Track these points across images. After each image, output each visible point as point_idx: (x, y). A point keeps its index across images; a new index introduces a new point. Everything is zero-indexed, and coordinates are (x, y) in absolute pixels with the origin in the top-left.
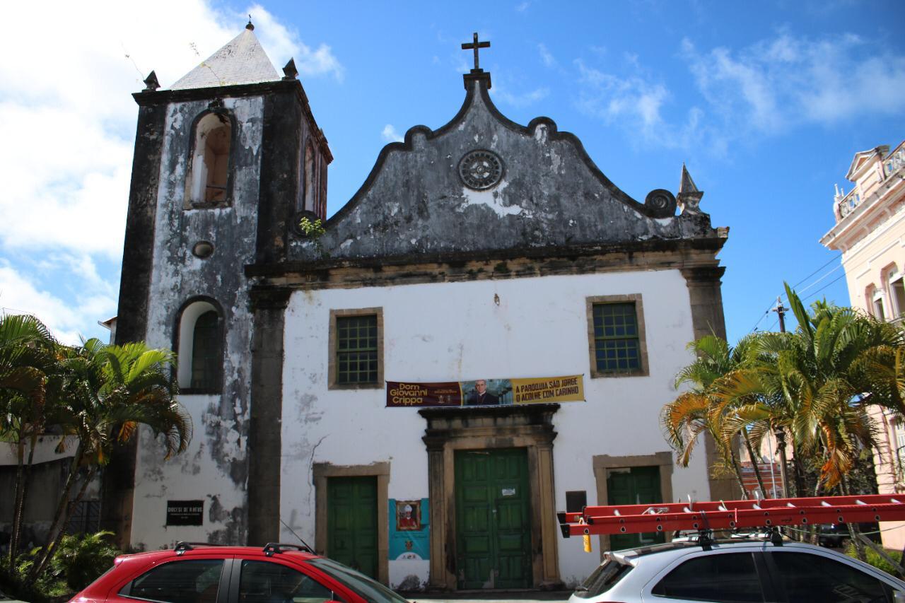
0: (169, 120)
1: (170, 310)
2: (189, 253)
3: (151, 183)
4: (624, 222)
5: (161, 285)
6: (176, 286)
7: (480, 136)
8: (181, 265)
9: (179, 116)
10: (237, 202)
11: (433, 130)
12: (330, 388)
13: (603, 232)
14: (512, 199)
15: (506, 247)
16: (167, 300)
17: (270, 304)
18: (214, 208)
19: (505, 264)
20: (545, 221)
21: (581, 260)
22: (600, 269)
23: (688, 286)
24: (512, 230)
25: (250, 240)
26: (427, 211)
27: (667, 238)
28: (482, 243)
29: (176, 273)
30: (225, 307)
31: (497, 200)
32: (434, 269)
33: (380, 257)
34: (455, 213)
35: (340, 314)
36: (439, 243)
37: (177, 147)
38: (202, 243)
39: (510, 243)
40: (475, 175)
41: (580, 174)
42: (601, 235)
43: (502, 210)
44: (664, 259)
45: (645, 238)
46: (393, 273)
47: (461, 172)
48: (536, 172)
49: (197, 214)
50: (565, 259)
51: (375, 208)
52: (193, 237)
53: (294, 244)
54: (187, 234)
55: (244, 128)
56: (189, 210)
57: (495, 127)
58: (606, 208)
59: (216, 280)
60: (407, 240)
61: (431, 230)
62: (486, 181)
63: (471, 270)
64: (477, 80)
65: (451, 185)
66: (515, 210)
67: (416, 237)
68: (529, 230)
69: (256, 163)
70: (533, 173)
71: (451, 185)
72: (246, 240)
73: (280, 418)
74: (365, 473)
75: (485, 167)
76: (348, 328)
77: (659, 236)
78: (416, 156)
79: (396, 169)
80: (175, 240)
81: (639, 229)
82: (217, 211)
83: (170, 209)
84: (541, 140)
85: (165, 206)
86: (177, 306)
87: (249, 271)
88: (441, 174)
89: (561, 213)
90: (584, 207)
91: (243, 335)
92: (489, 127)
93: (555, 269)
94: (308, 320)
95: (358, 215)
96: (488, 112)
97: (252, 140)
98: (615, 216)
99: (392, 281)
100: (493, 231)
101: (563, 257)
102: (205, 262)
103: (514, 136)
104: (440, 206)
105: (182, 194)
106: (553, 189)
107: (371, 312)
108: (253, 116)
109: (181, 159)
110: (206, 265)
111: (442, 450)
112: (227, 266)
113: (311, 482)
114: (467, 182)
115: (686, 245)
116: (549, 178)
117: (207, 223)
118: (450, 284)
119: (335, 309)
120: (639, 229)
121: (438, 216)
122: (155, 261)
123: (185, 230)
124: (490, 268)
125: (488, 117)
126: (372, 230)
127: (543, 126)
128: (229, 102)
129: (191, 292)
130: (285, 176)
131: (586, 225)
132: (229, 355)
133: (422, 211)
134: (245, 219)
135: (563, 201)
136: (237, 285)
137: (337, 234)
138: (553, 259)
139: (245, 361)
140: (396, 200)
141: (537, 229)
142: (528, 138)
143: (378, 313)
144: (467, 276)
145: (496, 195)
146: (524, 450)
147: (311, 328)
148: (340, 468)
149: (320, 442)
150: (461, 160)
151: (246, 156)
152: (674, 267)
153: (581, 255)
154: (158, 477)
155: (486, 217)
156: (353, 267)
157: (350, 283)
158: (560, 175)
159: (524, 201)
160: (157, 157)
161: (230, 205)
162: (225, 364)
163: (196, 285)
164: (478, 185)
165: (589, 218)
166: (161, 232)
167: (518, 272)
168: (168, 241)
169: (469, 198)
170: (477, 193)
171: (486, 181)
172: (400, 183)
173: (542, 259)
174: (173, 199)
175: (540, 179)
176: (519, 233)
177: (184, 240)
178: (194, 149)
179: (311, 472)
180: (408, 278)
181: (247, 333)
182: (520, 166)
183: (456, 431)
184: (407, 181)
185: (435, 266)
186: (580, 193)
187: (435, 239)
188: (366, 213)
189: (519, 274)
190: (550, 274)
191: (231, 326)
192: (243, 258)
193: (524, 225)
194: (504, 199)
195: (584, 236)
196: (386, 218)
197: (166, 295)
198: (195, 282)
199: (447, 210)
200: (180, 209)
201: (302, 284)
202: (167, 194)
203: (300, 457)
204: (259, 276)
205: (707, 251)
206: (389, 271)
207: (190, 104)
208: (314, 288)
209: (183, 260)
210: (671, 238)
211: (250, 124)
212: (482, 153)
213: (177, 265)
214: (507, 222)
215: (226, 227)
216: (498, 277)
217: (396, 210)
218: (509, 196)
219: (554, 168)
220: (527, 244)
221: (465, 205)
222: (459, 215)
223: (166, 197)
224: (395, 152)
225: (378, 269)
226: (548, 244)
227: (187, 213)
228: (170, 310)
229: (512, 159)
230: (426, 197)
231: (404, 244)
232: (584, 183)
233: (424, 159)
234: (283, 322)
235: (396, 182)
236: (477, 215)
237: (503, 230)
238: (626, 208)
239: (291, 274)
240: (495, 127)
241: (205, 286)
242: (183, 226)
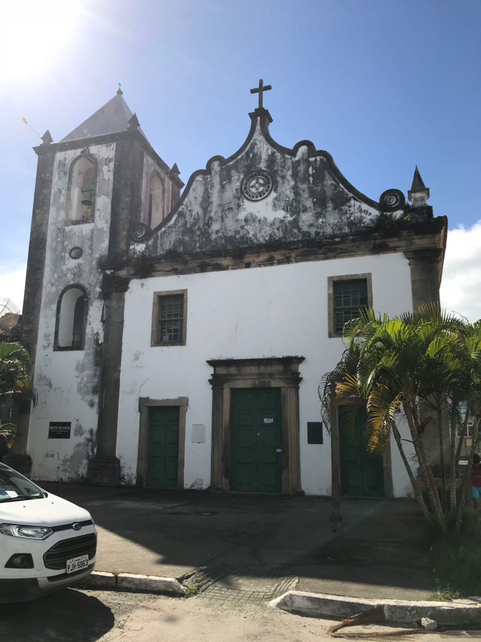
11: (226, 157)
12: (152, 346)
17: (114, 289)
73: (120, 366)
74: (171, 404)
94: (140, 300)
107: (180, 293)
111: (223, 389)
113: (137, 410)
130: (128, 199)
143: (185, 294)
146: (279, 389)
148: (156, 401)
149: (144, 382)
152: (400, 251)
179: (138, 402)
180: (203, 268)
183: (231, 375)
203: (132, 392)
225: (186, 262)
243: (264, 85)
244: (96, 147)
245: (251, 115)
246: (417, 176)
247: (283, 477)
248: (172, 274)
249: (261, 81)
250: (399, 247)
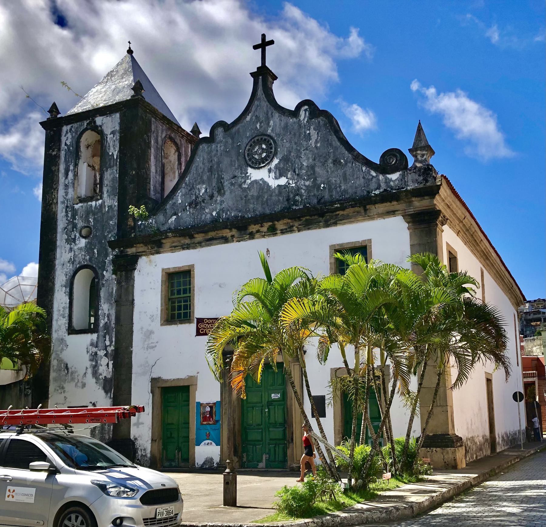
1: (68, 276)
2: (78, 235)
3: (54, 187)
4: (362, 180)
5: (62, 259)
6: (71, 259)
7: (260, 124)
8: (73, 244)
10: (105, 195)
11: (229, 123)
13: (345, 191)
14: (281, 172)
15: (275, 212)
16: (66, 270)
17: (126, 267)
18: (91, 202)
19: (274, 225)
20: (304, 188)
21: (327, 216)
22: (340, 222)
23: (409, 229)
24: (280, 198)
26: (223, 189)
27: (395, 190)
28: (259, 209)
29: (71, 250)
30: (99, 272)
31: (271, 174)
32: (227, 233)
33: (193, 227)
34: (242, 188)
35: (168, 271)
36: (231, 213)
37: (69, 159)
38: (85, 227)
39: (278, 208)
40: (256, 157)
41: (331, 145)
42: (344, 194)
43: (273, 183)
44: (392, 208)
45: (377, 192)
46: (201, 238)
47: (246, 155)
48: (299, 148)
49: (82, 207)
50: (316, 217)
51: (190, 191)
52: (80, 224)
53: (140, 222)
54: (76, 221)
55: (108, 139)
56: (77, 204)
57: (272, 113)
58: (349, 171)
59: (94, 253)
60: (211, 212)
61: (225, 204)
62: (263, 160)
63: (252, 232)
65: (240, 167)
66: (283, 181)
67: (216, 210)
68: (291, 196)
70: (297, 149)
71: (240, 167)
75: (263, 149)
76: (176, 281)
77: (388, 189)
78: (217, 147)
79: (204, 159)
80: (70, 227)
81: (373, 185)
82: (93, 203)
84: (304, 120)
85: (63, 203)
86: (72, 273)
87: (113, 245)
88: (234, 159)
89: (315, 179)
90: (332, 172)
91: (110, 291)
92: (267, 114)
93: (308, 225)
95: (179, 197)
96: (267, 103)
98: (355, 176)
99: (200, 244)
100: (267, 199)
101: (314, 215)
102: (87, 240)
104: (232, 184)
105: (73, 193)
106: (311, 160)
107: (187, 268)
108: (113, 129)
109: (71, 168)
112: (100, 243)
114: (250, 163)
115: (406, 195)
116: (308, 152)
117: (89, 212)
118: (237, 243)
119: (165, 268)
120: (373, 185)
121: (231, 193)
122: (58, 243)
124: (265, 229)
125: (267, 106)
126: (188, 208)
127: (306, 107)
129: (79, 263)
131: (333, 187)
132: (102, 305)
133: (220, 190)
134: (110, 207)
135: (317, 169)
136: (107, 255)
137: (166, 213)
138: (307, 218)
139: (112, 309)
140: (203, 183)
141: (297, 195)
142: (295, 119)
144: (248, 236)
145: (270, 171)
147: (150, 283)
150: (247, 145)
151: (110, 160)
153: (327, 212)
155: (263, 189)
156: (174, 237)
157: (174, 248)
158: (316, 147)
159: (290, 173)
160: (57, 168)
161: (101, 198)
162: (100, 312)
163: (82, 257)
164: (257, 165)
165: (335, 181)
166: (61, 223)
167: (281, 230)
168: (66, 228)
169: (251, 175)
170: (257, 171)
171: (266, 159)
172: (206, 170)
173: (299, 218)
174: (67, 197)
175: (301, 153)
176: (285, 199)
177: (75, 226)
178: (79, 159)
180: (210, 241)
181: (113, 289)
182: (288, 145)
184: (211, 167)
185: (228, 231)
186: (330, 161)
187: (228, 210)
188: (184, 195)
189: (283, 232)
190: (305, 230)
191: (103, 284)
192: (110, 236)
193: (288, 193)
194: (275, 173)
195: (331, 196)
196: (197, 197)
197: (65, 266)
199: (236, 187)
201: (144, 252)
204: (119, 248)
205: (426, 198)
206: (199, 237)
208: (153, 254)
209: (74, 240)
210: (398, 189)
211: (112, 135)
212: (263, 138)
214: (277, 191)
215: (99, 214)
216: (269, 236)
217: (203, 191)
218: (279, 170)
219: (312, 142)
220: (290, 208)
221: (249, 181)
222: (245, 190)
223: (63, 196)
224: (204, 145)
225: (192, 237)
226: (305, 206)
227: (76, 207)
228: (68, 276)
229: (282, 140)
230: (223, 178)
231: (208, 216)
232: (334, 152)
233: (222, 148)
234: (134, 280)
235: (204, 169)
236: (257, 188)
237: (274, 198)
238: (364, 169)
239: (138, 245)
240: (272, 113)
241: (88, 257)
242: (74, 217)
243: (267, 40)
244: (101, 118)
245: (252, 74)
246: (420, 130)
247: (289, 452)
248: (179, 250)
249: (264, 36)
250: (397, 211)
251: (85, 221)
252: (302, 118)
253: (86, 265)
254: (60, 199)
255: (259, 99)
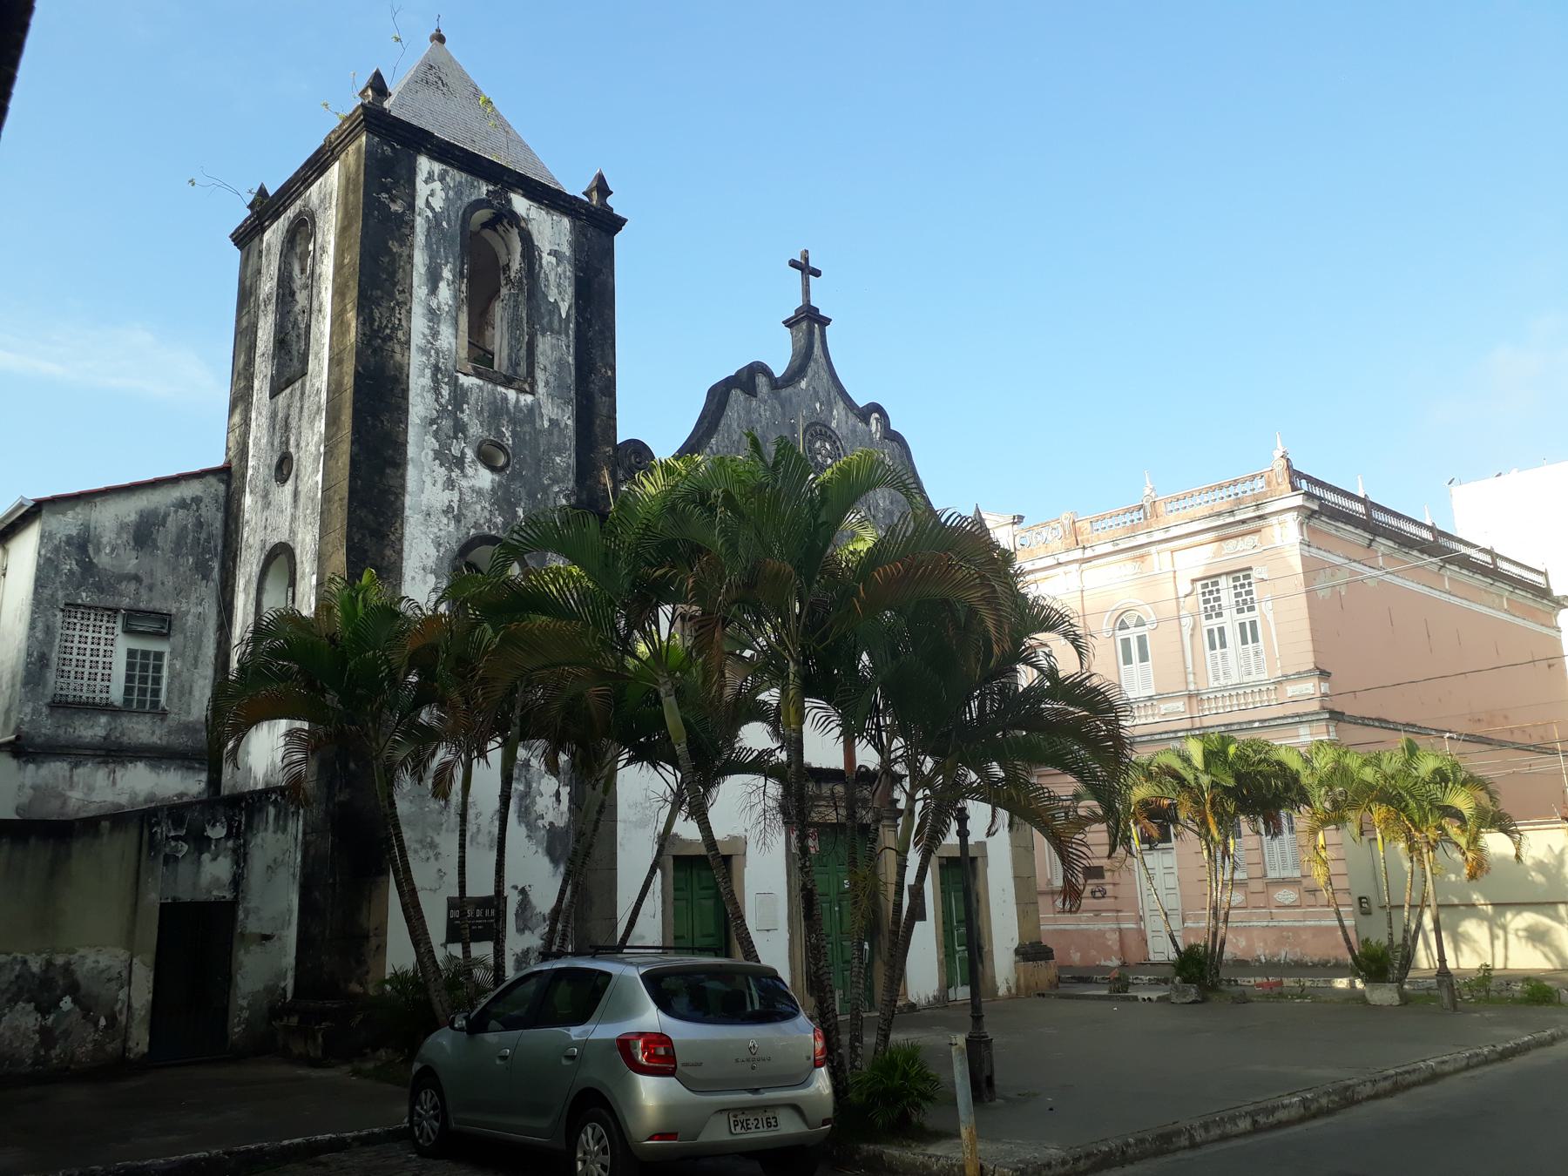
0: (422, 190)
1: (442, 550)
5: (424, 498)
6: (450, 506)
9: (437, 185)
10: (541, 389)
18: (507, 387)
25: (564, 461)
49: (480, 388)
52: (476, 429)
55: (544, 262)
64: (809, 321)
69: (567, 336)
72: (558, 460)
80: (446, 423)
82: (512, 394)
83: (432, 360)
97: (560, 294)
103: (853, 420)
105: (453, 340)
110: (500, 484)
112: (531, 496)
122: (411, 451)
123: (462, 412)
128: (520, 204)
129: (476, 525)
151: (551, 313)
154: (431, 854)
160: (406, 252)
161: (532, 393)
163: (482, 516)
168: (433, 422)
174: (438, 344)
177: (460, 428)
192: (556, 489)
198: (483, 508)
200: (450, 367)
202: (427, 331)
203: (642, 824)
207: (456, 176)
209: (460, 462)
211: (554, 260)
213: (450, 470)
215: (527, 428)
227: (463, 379)
241: (499, 520)
251: (489, 424)
252: (874, 429)
253: (494, 537)
254: (417, 340)
255: (816, 361)
